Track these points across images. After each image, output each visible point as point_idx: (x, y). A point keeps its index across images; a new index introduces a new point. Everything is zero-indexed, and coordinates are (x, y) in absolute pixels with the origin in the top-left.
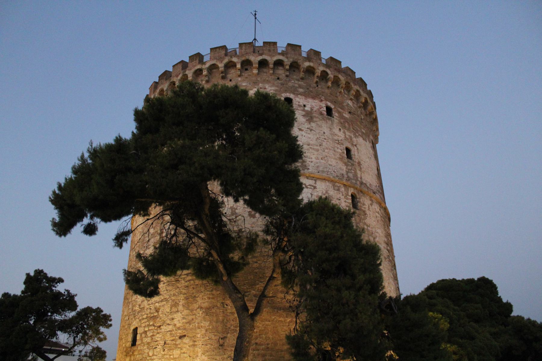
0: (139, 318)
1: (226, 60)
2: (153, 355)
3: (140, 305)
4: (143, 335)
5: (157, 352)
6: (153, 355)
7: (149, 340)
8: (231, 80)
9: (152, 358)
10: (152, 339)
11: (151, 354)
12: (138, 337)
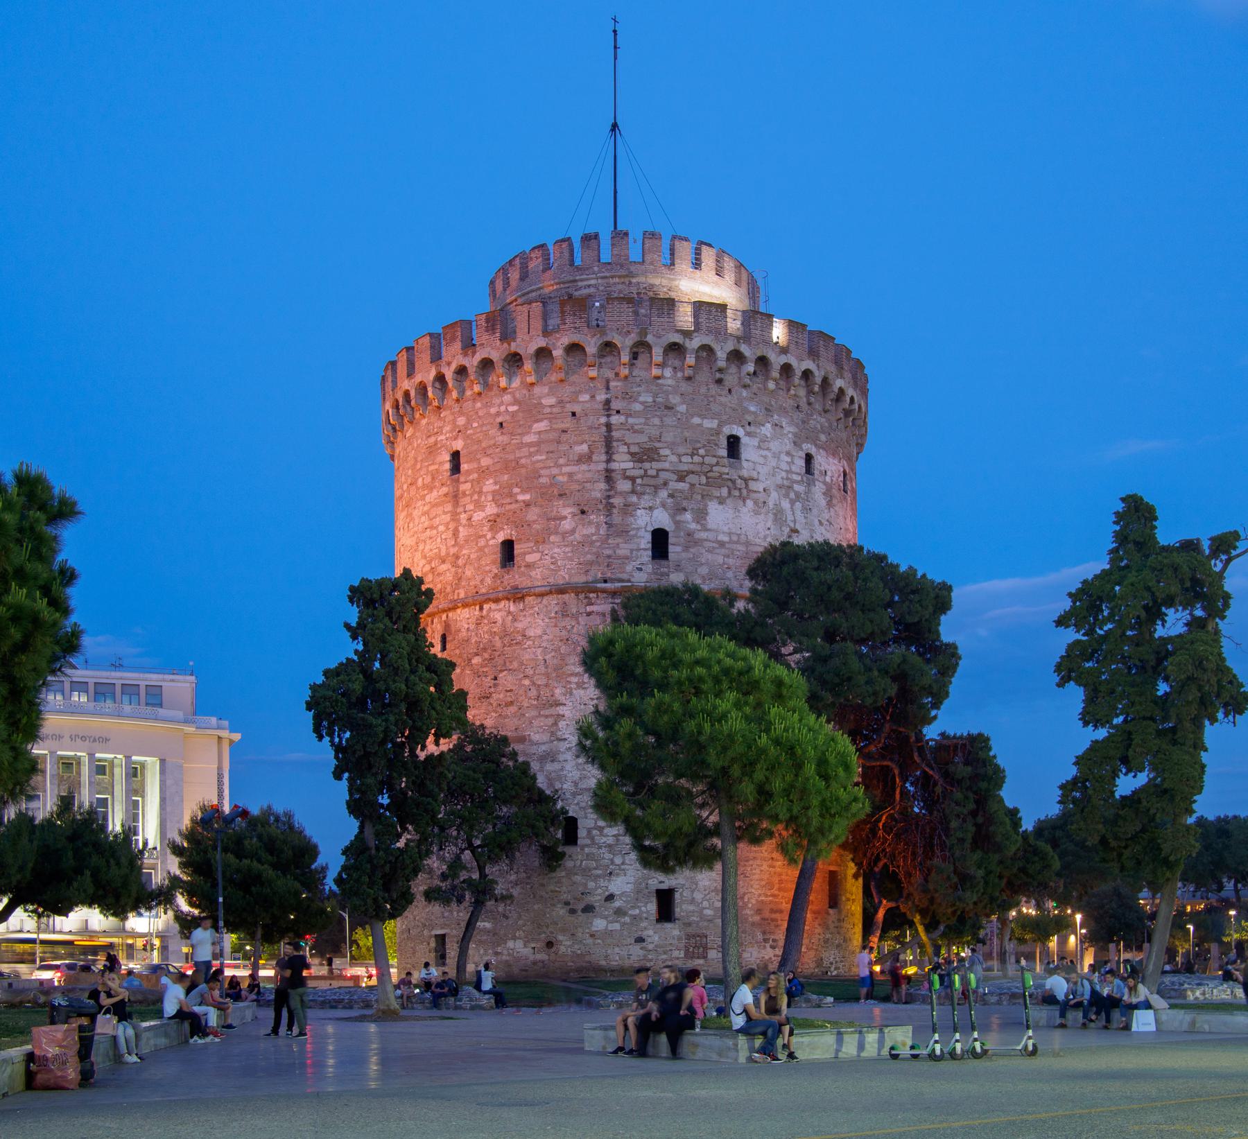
0: (578, 804)
1: (730, 346)
2: (623, 863)
3: (576, 784)
4: (595, 832)
5: (631, 860)
6: (623, 863)
7: (611, 841)
8: (730, 391)
9: (623, 867)
10: (618, 840)
11: (618, 860)
12: (582, 833)
